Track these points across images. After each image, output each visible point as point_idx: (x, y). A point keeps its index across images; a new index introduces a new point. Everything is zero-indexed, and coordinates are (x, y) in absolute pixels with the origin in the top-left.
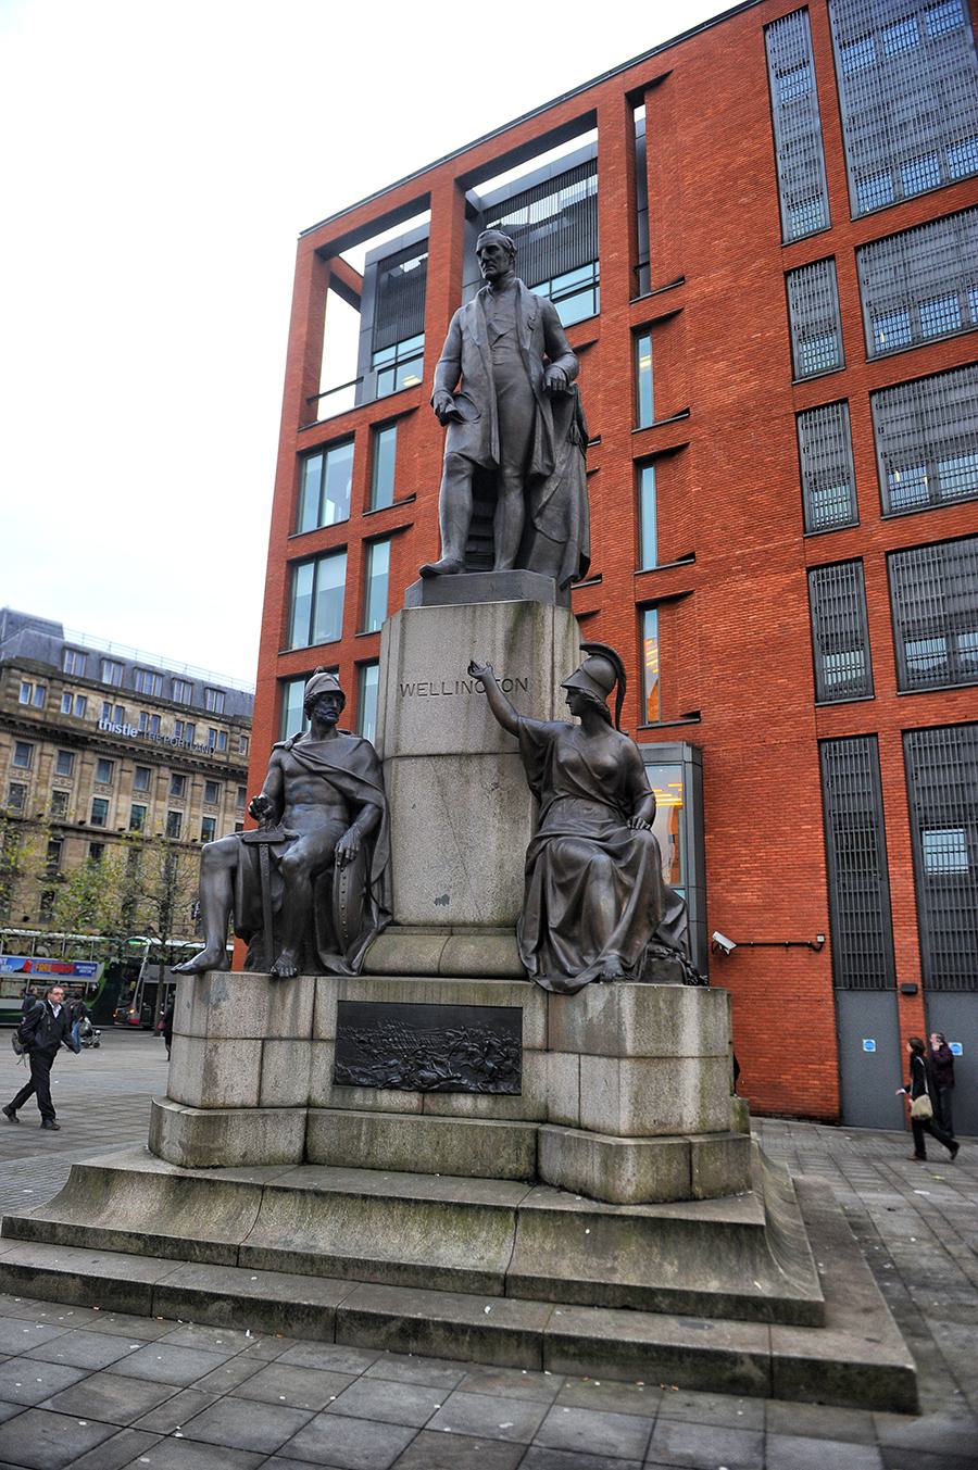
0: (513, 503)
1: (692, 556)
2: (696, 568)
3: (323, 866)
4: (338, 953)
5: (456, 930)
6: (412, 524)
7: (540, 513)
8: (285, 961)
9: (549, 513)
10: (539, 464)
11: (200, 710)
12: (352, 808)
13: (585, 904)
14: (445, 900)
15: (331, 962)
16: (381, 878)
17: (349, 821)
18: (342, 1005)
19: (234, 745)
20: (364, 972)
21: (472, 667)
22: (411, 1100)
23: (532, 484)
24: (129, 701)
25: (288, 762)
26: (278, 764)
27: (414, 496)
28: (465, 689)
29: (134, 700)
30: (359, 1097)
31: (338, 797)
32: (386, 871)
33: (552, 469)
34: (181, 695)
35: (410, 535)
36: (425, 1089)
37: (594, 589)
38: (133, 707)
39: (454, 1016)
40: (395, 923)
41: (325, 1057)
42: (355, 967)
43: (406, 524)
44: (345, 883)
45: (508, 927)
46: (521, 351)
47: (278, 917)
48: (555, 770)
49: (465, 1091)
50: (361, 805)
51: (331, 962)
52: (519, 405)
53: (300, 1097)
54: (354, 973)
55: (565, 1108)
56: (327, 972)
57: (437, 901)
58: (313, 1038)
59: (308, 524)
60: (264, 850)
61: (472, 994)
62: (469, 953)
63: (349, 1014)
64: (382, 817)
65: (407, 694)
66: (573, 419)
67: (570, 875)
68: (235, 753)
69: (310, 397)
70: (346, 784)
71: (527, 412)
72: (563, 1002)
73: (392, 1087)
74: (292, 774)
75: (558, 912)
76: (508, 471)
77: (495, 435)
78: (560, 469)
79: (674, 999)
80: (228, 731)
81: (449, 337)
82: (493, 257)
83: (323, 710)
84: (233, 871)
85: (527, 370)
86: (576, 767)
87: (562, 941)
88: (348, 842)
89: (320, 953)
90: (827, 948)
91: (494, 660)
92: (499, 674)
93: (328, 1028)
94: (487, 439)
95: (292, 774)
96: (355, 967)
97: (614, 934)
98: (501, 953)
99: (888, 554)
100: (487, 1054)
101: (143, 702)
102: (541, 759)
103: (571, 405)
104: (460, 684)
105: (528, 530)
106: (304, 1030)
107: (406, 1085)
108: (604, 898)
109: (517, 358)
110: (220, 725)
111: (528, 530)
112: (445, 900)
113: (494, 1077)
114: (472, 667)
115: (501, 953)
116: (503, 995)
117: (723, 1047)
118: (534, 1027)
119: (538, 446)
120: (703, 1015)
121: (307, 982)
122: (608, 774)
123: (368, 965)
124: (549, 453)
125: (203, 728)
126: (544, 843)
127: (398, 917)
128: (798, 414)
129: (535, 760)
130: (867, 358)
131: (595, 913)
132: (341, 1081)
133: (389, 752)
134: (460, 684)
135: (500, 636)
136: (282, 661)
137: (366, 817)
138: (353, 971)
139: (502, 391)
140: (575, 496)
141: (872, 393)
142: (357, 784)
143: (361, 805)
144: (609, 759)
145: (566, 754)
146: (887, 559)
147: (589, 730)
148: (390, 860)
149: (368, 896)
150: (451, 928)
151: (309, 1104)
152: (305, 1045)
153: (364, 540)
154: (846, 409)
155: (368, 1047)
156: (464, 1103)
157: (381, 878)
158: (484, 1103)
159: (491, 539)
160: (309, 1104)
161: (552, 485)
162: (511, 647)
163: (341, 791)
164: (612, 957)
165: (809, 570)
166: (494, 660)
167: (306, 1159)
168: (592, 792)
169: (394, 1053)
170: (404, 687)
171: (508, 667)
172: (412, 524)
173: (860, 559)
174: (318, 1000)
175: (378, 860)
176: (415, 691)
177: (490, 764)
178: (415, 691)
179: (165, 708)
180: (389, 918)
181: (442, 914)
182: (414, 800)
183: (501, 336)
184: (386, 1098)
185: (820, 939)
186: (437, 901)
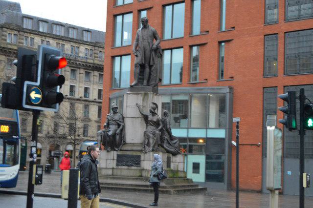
0: (147, 70)
1: (234, 28)
2: (235, 32)
3: (114, 135)
6: (153, 7)
7: (152, 71)
8: (109, 149)
9: (154, 71)
10: (151, 64)
11: (80, 40)
12: (119, 125)
14: (133, 140)
17: (119, 127)
19: (96, 55)
20: (121, 150)
21: (137, 104)
22: (126, 167)
23: (151, 67)
24: (51, 39)
25: (109, 118)
29: (53, 38)
30: (120, 167)
33: (154, 63)
34: (73, 34)
35: (152, 10)
36: (128, 166)
37: (206, 36)
38: (53, 41)
39: (132, 156)
40: (126, 143)
41: (115, 162)
44: (118, 137)
46: (148, 42)
47: (108, 143)
49: (133, 166)
50: (120, 125)
52: (148, 52)
55: (145, 168)
56: (115, 150)
58: (113, 159)
61: (134, 153)
62: (135, 148)
63: (118, 156)
64: (124, 127)
69: (115, 14)
70: (118, 122)
71: (149, 54)
72: (145, 154)
75: (146, 142)
76: (146, 64)
77: (144, 59)
78: (156, 63)
80: (93, 49)
81: (136, 36)
83: (114, 110)
84: (101, 136)
85: (149, 45)
86: (151, 121)
88: (118, 131)
90: (261, 146)
91: (140, 103)
92: (141, 104)
93: (115, 158)
94: (142, 59)
97: (152, 145)
98: (139, 148)
99: (285, 33)
100: (137, 161)
101: (57, 39)
103: (158, 50)
105: (150, 74)
106: (112, 158)
107: (126, 165)
108: (151, 141)
109: (148, 44)
110: (90, 46)
111: (150, 74)
112: (133, 140)
113: (137, 164)
114: (137, 104)
116: (138, 153)
117: (166, 160)
118: (142, 158)
121: (112, 152)
122: (155, 122)
124: (153, 59)
125: (82, 48)
127: (127, 142)
132: (117, 165)
136: (113, 50)
137: (121, 127)
140: (158, 68)
143: (120, 125)
144: (155, 120)
145: (149, 119)
146: (285, 35)
147: (153, 115)
149: (121, 139)
155: (120, 160)
156: (133, 168)
159: (143, 75)
161: (154, 66)
162: (143, 100)
164: (151, 149)
166: (140, 103)
167: (113, 175)
171: (143, 103)
172: (153, 7)
173: (277, 34)
174: (114, 154)
175: (123, 134)
177: (140, 119)
179: (66, 40)
182: (128, 123)
184: (124, 167)
185: (259, 143)
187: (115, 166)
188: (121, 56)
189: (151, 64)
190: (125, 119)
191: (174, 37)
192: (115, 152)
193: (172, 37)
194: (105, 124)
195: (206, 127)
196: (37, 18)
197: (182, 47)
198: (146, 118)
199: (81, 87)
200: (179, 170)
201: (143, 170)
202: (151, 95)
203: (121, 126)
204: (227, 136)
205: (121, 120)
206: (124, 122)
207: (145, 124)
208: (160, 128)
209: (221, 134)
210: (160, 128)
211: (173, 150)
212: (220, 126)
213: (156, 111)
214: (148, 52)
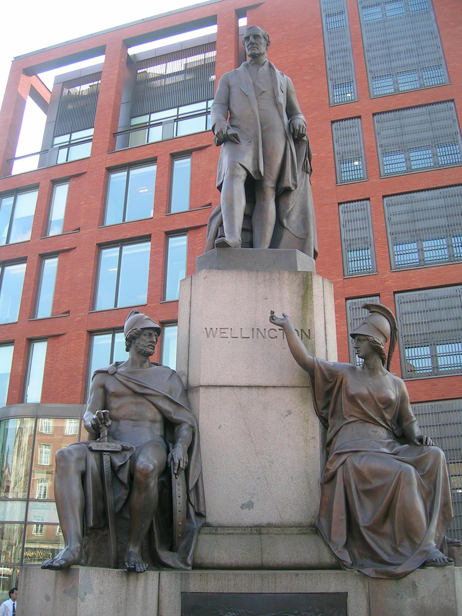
4: (172, 548)
5: (264, 531)
10: (288, 181)
13: (398, 505)
14: (249, 505)
15: (165, 556)
16: (196, 485)
18: (185, 595)
20: (196, 567)
23: (282, 193)
27: (79, 229)
28: (260, 335)
31: (159, 417)
32: (200, 478)
40: (207, 525)
42: (190, 562)
43: (71, 247)
45: (315, 529)
48: (344, 400)
50: (179, 423)
51: (165, 556)
54: (190, 568)
57: (243, 507)
60: (106, 458)
62: (283, 551)
64: (194, 432)
65: (211, 336)
66: (306, 156)
67: (376, 483)
70: (166, 406)
74: (117, 395)
82: (257, 42)
83: (143, 342)
87: (373, 536)
89: (158, 550)
95: (117, 395)
96: (190, 562)
99: (395, 293)
102: (329, 393)
104: (255, 330)
105: (279, 224)
115: (308, 550)
116: (329, 583)
121: (153, 575)
123: (198, 561)
126: (343, 458)
128: (339, 204)
129: (324, 391)
130: (381, 176)
131: (408, 512)
133: (193, 382)
134: (255, 330)
137: (184, 432)
138: (188, 565)
139: (265, 127)
141: (384, 197)
142: (174, 406)
143: (179, 423)
146: (394, 295)
150: (258, 530)
154: (368, 204)
157: (196, 485)
163: (160, 410)
165: (347, 299)
168: (377, 419)
170: (208, 330)
176: (218, 333)
178: (218, 333)
180: (203, 521)
182: (217, 422)
183: (263, 92)
186: (243, 507)
191: (119, 306)
192: (165, 575)
193: (116, 305)
203: (185, 427)
206: (189, 407)
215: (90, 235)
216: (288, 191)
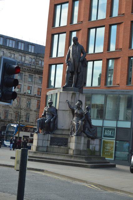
3: (49, 122)
4: (51, 132)
10: (79, 72)
11: (27, 52)
15: (50, 132)
17: (53, 117)
19: (37, 63)
20: (53, 134)
21: (67, 101)
22: (57, 146)
24: (5, 49)
26: (45, 110)
29: (7, 49)
30: (52, 146)
33: (81, 71)
34: (21, 47)
35: (81, 32)
36: (59, 145)
38: (7, 51)
39: (62, 139)
41: (49, 142)
43: (80, 29)
44: (52, 125)
51: (50, 132)
52: (77, 63)
53: (46, 146)
59: (57, 25)
61: (64, 137)
62: (64, 133)
63: (51, 138)
64: (57, 117)
68: (38, 65)
70: (52, 113)
73: (56, 145)
77: (73, 67)
79: (81, 138)
80: (36, 58)
91: (69, 99)
93: (49, 139)
94: (72, 68)
101: (9, 50)
106: (47, 139)
110: (33, 56)
113: (65, 145)
116: (66, 137)
117: (86, 143)
119: (79, 69)
120: (84, 140)
121: (47, 135)
124: (80, 69)
125: (28, 57)
132: (51, 144)
133: (58, 109)
135: (71, 97)
137: (54, 117)
148: (57, 122)
151: (47, 147)
152: (47, 141)
153: (70, 31)
156: (62, 147)
158: (64, 147)
160: (47, 147)
161: (81, 73)
162: (72, 98)
166: (69, 99)
169: (56, 142)
174: (49, 136)
179: (16, 51)
181: (62, 128)
182: (60, 114)
184: (55, 146)
187: (49, 145)
188: (56, 64)
189: (79, 72)
190: (58, 111)
193: (94, 52)
194: (43, 114)
195: (117, 119)
196: (27, 42)
197: (101, 60)
198: (73, 111)
199: (25, 86)
200: (96, 150)
201: (69, 149)
202: (78, 95)
204: (132, 127)
205: (55, 112)
207: (72, 116)
208: (83, 119)
209: (128, 125)
210: (83, 119)
211: (91, 136)
212: (126, 119)
213: (81, 106)
214: (77, 63)
215: (86, 25)
216: (79, 73)
